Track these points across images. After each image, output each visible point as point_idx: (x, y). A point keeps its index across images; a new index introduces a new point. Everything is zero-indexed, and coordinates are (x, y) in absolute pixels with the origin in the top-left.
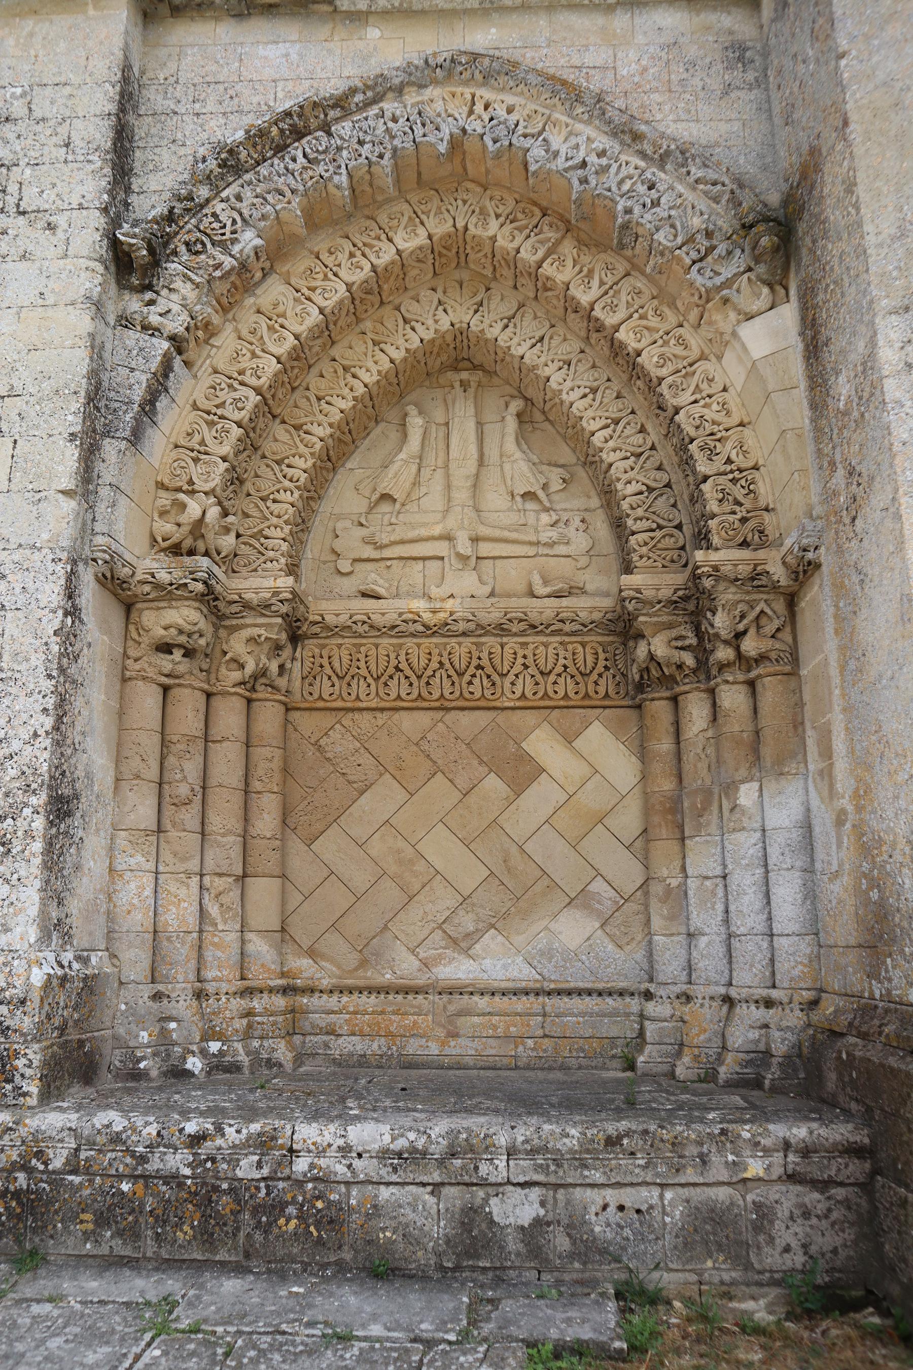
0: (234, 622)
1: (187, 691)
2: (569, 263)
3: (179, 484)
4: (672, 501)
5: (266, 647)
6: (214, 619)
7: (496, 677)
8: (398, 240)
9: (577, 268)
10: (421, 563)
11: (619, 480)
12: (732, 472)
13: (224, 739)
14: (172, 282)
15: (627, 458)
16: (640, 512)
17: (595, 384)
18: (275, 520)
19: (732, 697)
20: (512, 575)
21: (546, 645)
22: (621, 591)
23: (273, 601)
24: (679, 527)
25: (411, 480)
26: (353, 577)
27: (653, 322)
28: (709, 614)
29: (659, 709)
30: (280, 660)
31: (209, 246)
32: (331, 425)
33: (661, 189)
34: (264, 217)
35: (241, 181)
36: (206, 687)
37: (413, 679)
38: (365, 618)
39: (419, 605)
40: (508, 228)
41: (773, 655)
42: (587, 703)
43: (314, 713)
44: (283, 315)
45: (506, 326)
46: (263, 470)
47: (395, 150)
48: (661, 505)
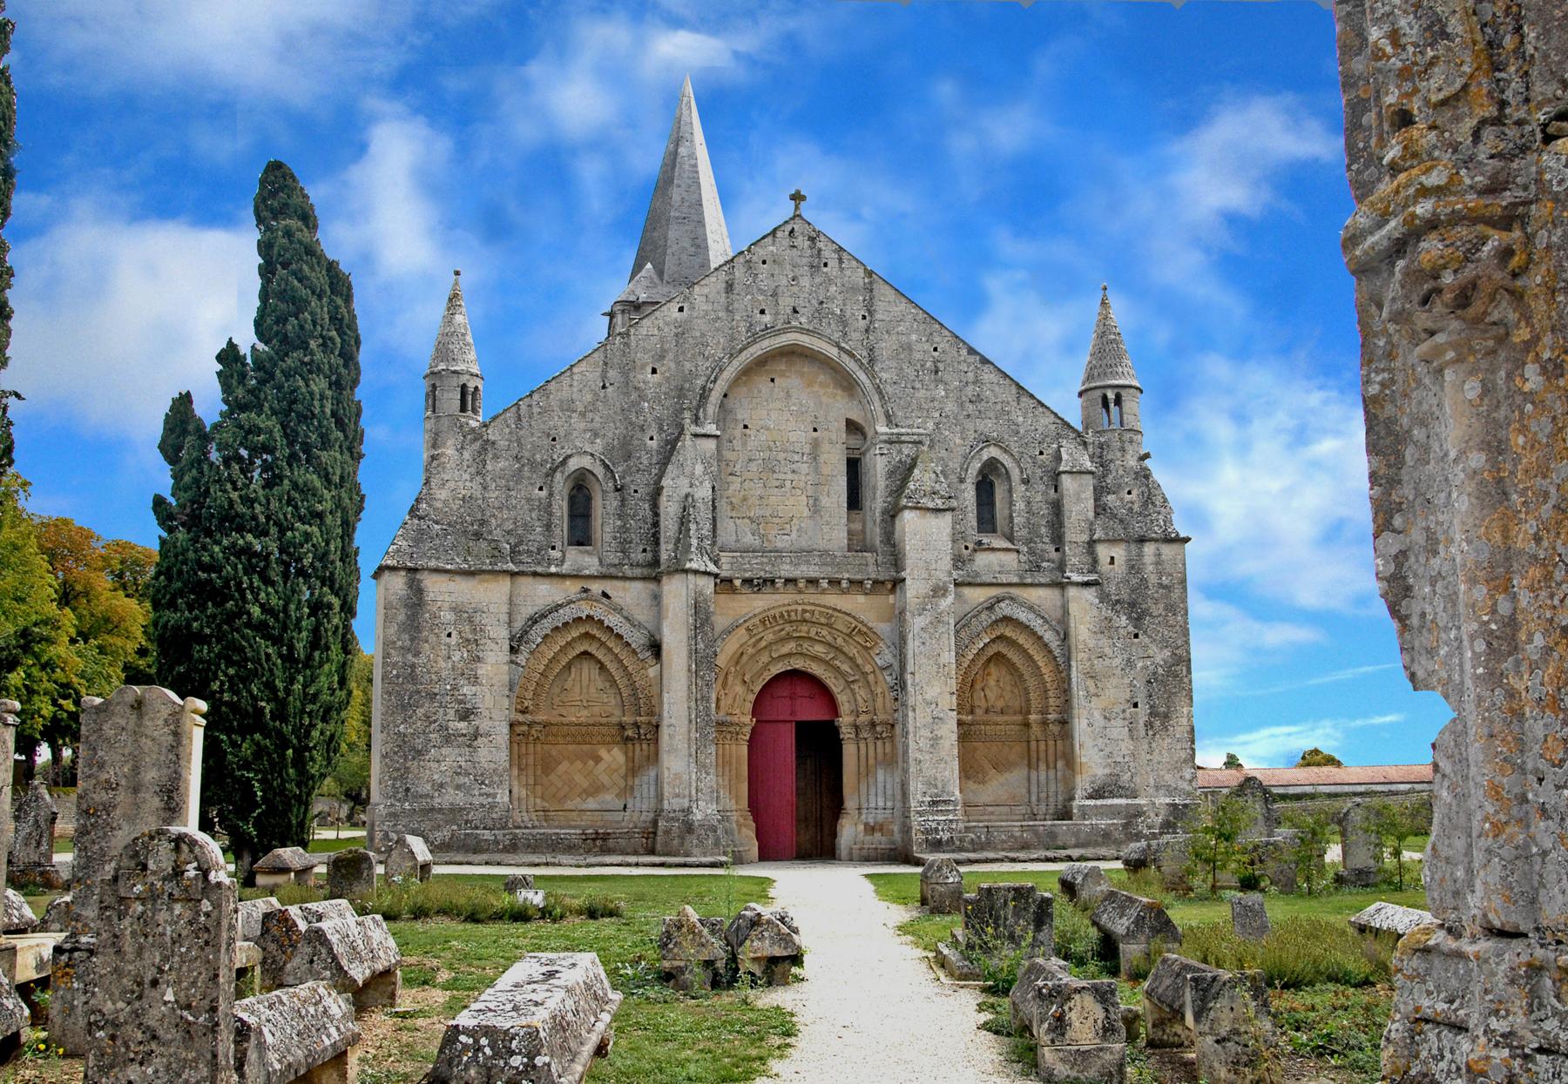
20: (596, 710)
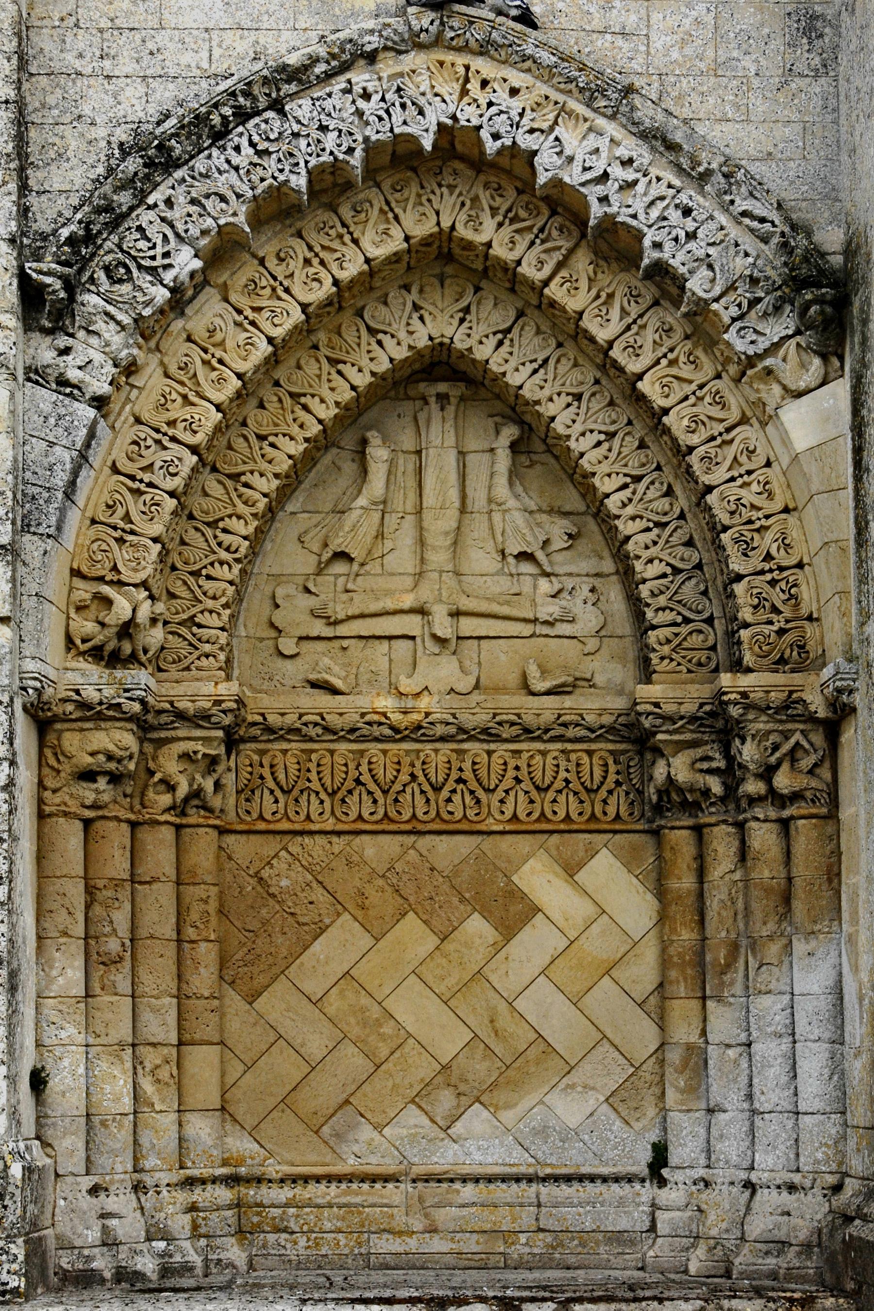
0: (163, 734)
1: (112, 824)
2: (584, 284)
3: (103, 573)
4: (702, 587)
5: (202, 765)
6: (141, 734)
7: (481, 794)
8: (365, 243)
9: (594, 292)
10: (385, 644)
11: (638, 557)
12: (771, 571)
13: (154, 880)
14: (91, 322)
15: (648, 529)
16: (662, 600)
17: (612, 428)
18: (210, 604)
19: (763, 837)
20: (502, 660)
21: (544, 753)
22: (636, 704)
23: (214, 711)
24: (710, 621)
25: (374, 533)
26: (299, 661)
27: (685, 371)
28: (737, 741)
29: (680, 839)
30: (216, 776)
31: (135, 271)
32: (277, 476)
33: (699, 218)
34: (204, 233)
35: (170, 181)
36: (132, 817)
37: (378, 794)
38: (318, 719)
39: (386, 703)
40: (507, 231)
42: (593, 826)
43: (252, 837)
44: (221, 344)
45: (500, 343)
46: (192, 536)
47: (366, 139)
48: (689, 591)
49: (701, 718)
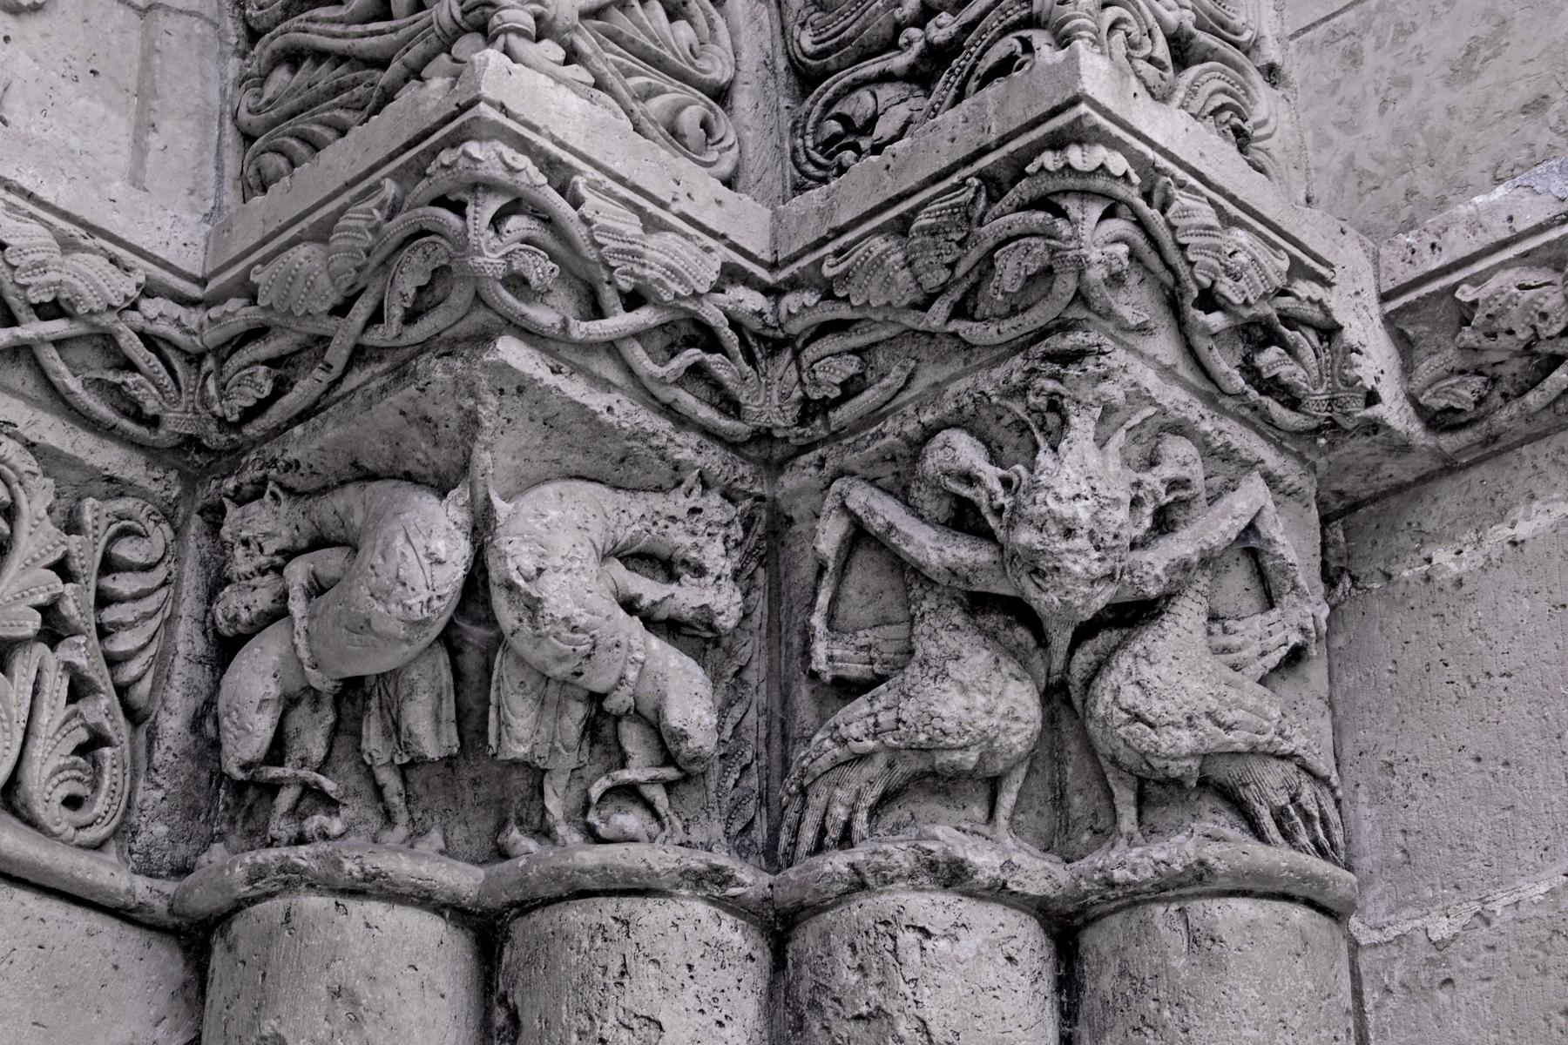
41: (1270, 786)
49: (707, 338)
